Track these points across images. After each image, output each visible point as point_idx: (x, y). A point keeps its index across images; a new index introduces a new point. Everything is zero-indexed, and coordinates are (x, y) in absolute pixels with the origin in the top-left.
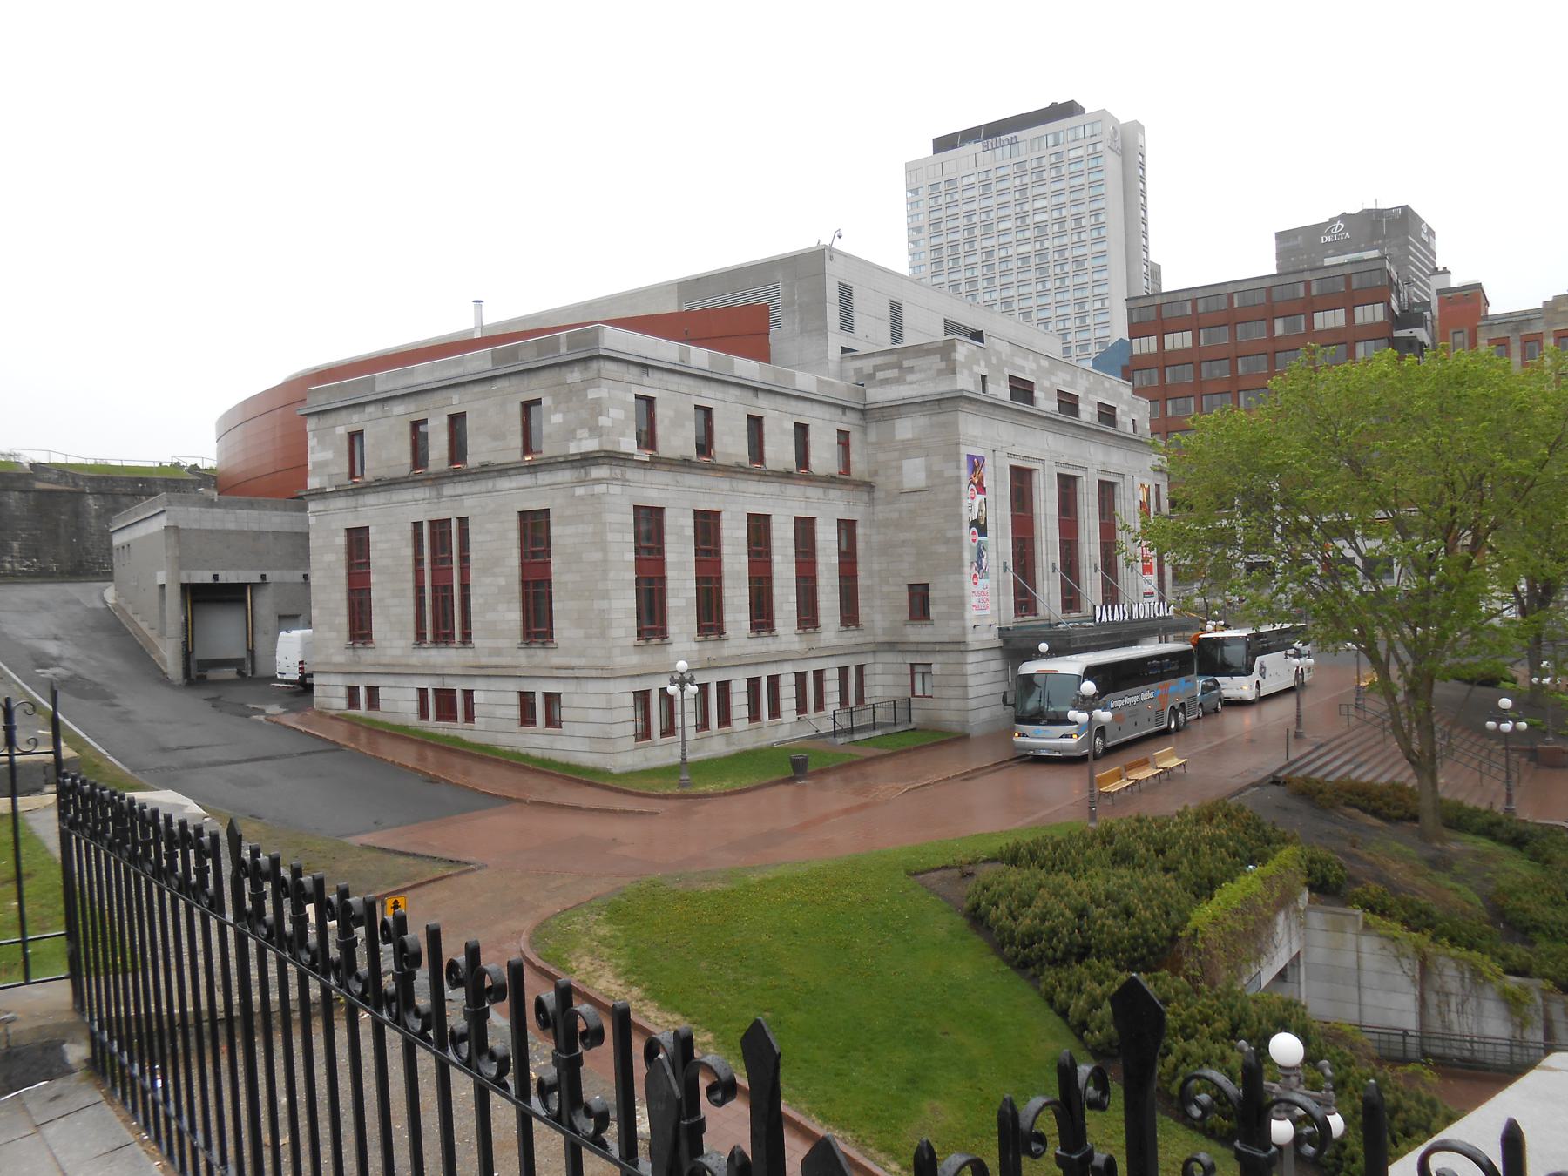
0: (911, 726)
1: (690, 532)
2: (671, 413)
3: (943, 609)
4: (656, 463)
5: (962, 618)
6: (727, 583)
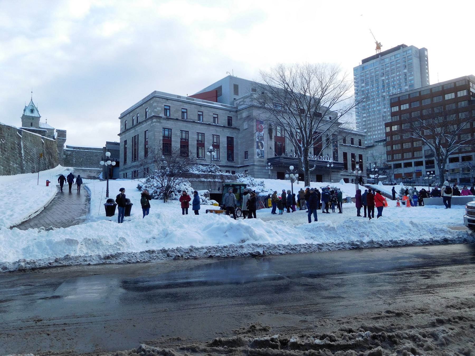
4: (168, 119)
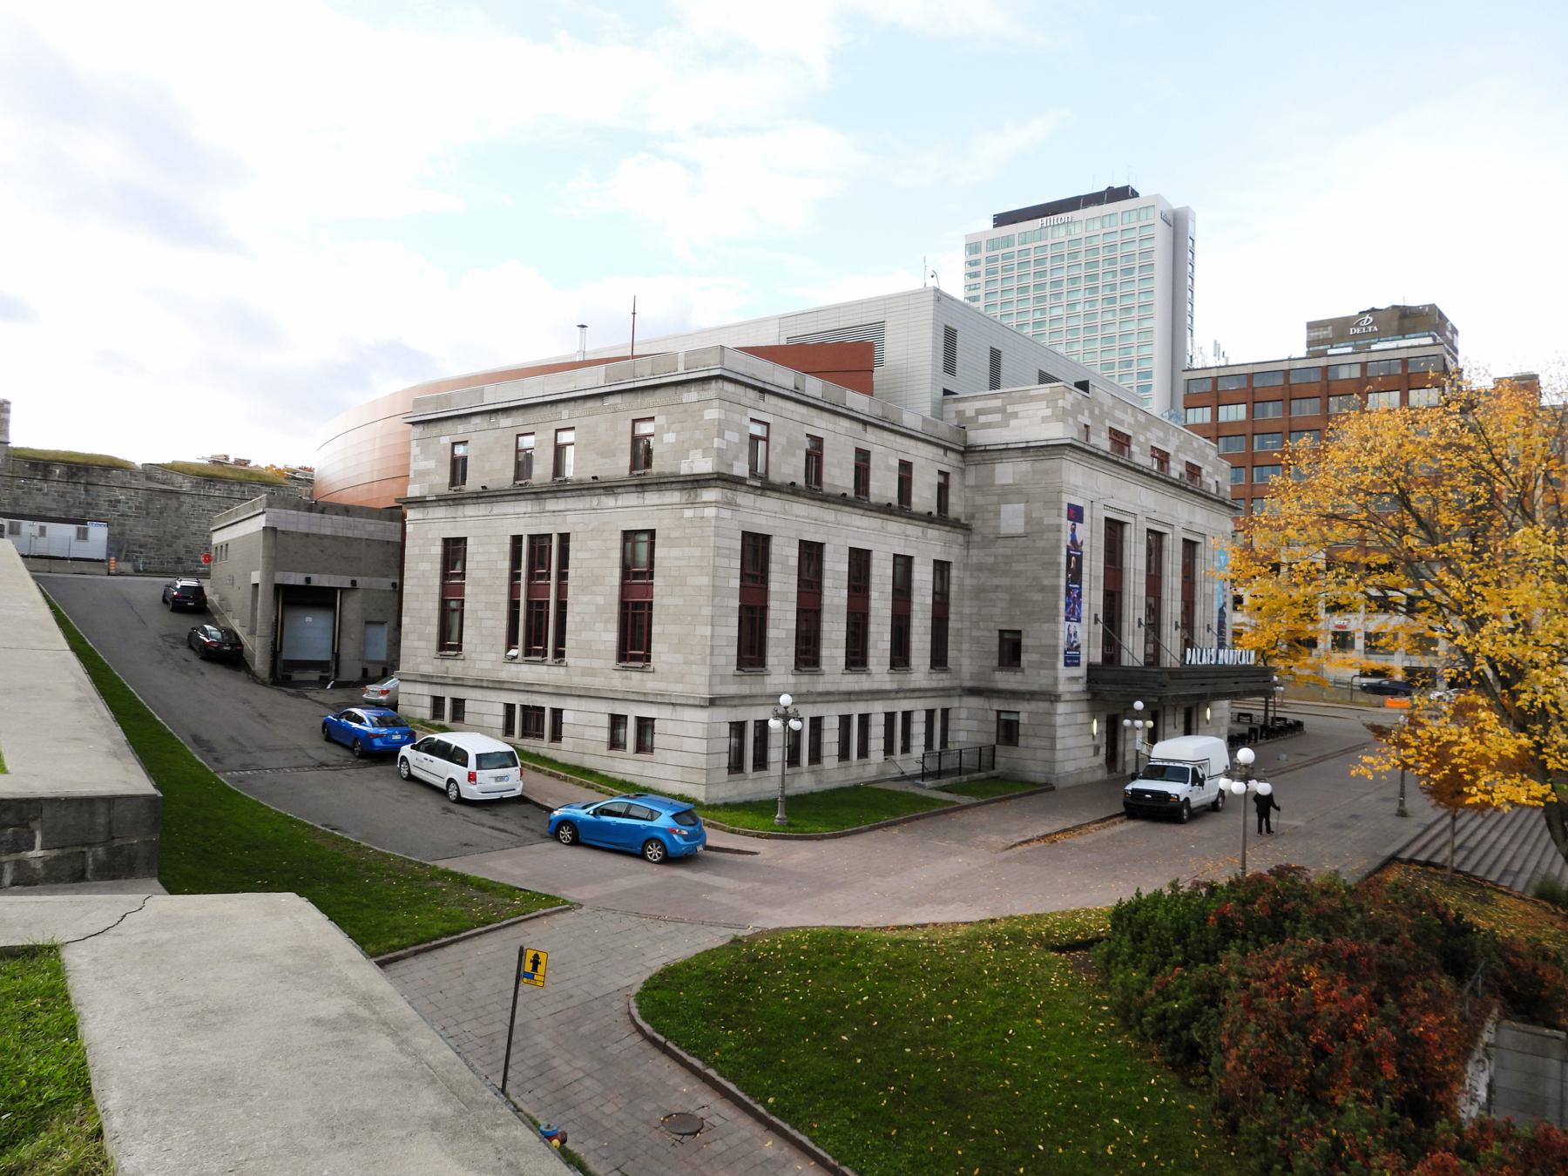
0: (993, 773)
1: (794, 562)
2: (783, 440)
3: (1035, 657)
5: (1054, 667)
6: (826, 617)
